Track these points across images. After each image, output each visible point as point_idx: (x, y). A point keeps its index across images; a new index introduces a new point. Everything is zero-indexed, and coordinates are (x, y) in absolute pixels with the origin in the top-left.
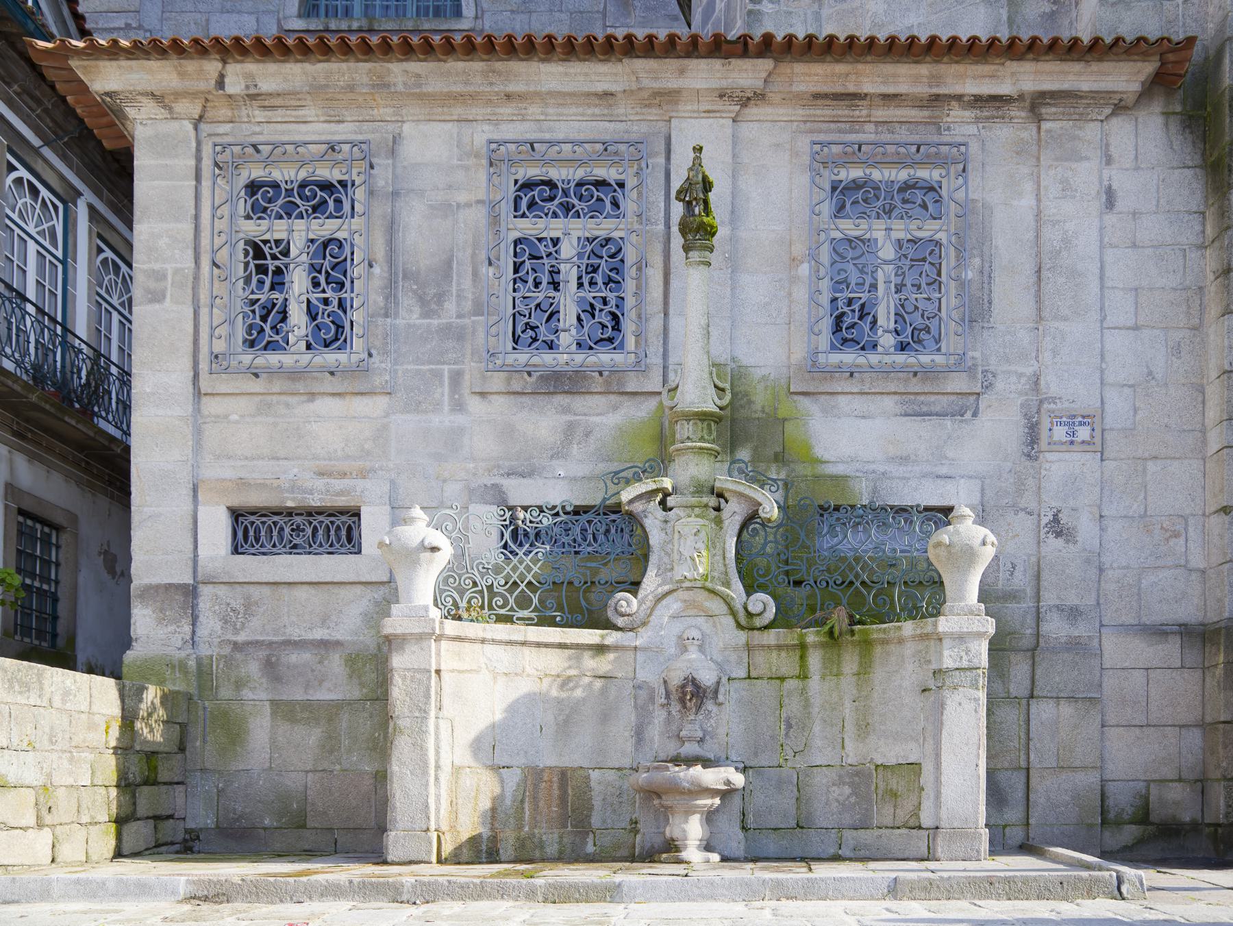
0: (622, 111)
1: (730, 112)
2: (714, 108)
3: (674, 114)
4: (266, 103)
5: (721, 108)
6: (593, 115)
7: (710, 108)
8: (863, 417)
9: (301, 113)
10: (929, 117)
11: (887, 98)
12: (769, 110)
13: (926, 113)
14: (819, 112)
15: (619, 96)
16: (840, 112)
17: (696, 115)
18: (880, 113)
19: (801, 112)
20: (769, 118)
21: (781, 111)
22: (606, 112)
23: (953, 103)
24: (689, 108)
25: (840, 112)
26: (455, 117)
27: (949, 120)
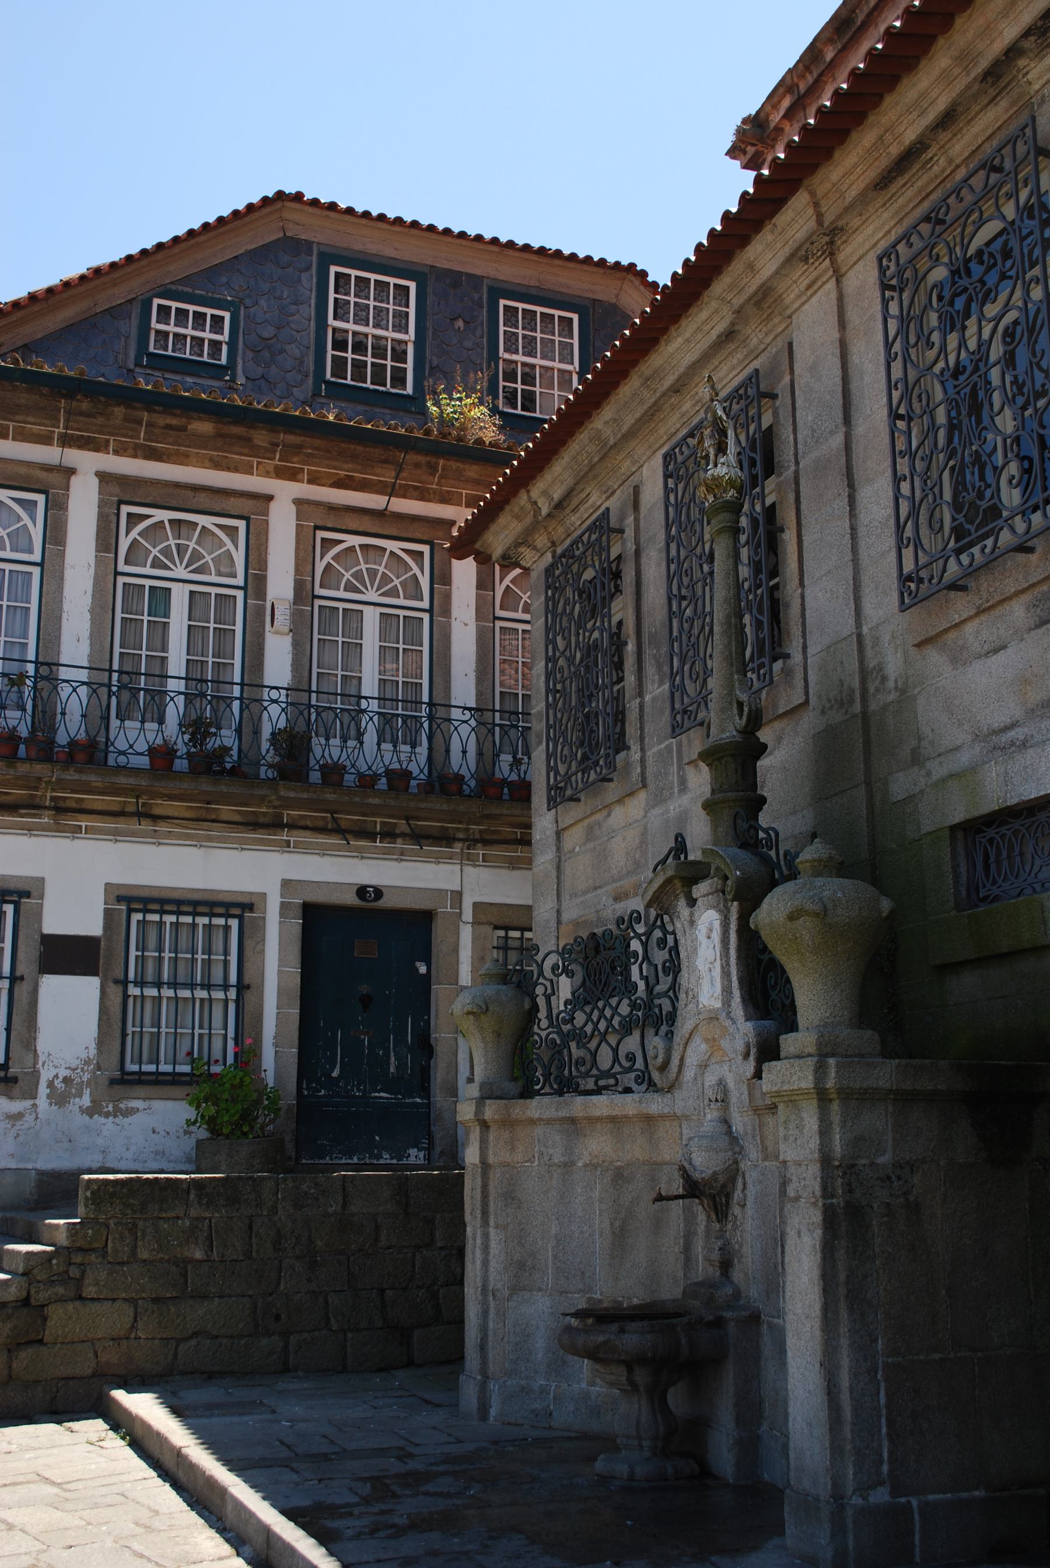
0: (755, 341)
1: (825, 271)
2: (811, 278)
3: (788, 312)
4: (572, 507)
5: (815, 274)
6: (740, 362)
7: (807, 282)
8: (996, 651)
9: (590, 502)
10: (1013, 104)
11: (947, 120)
12: (859, 238)
13: (1003, 104)
14: (901, 201)
15: (736, 328)
16: (920, 184)
17: (804, 298)
18: (958, 148)
19: (886, 215)
20: (867, 247)
21: (870, 230)
22: (745, 351)
23: (1021, 63)
24: (792, 296)
25: (920, 184)
26: (665, 438)
27: (1037, 87)
